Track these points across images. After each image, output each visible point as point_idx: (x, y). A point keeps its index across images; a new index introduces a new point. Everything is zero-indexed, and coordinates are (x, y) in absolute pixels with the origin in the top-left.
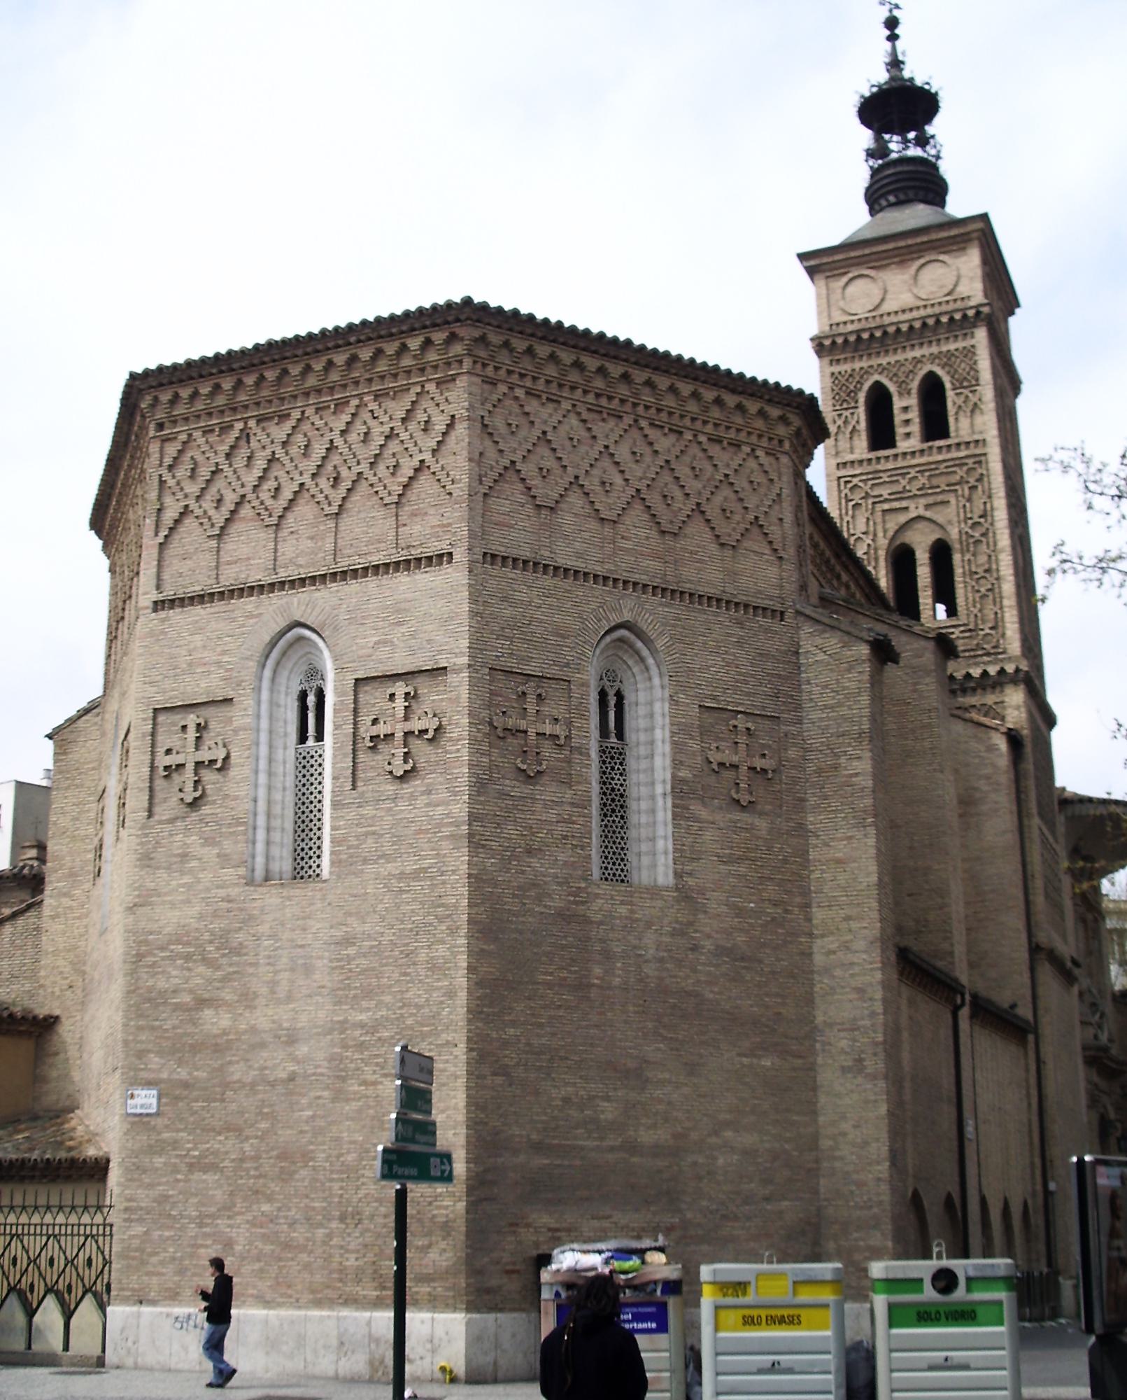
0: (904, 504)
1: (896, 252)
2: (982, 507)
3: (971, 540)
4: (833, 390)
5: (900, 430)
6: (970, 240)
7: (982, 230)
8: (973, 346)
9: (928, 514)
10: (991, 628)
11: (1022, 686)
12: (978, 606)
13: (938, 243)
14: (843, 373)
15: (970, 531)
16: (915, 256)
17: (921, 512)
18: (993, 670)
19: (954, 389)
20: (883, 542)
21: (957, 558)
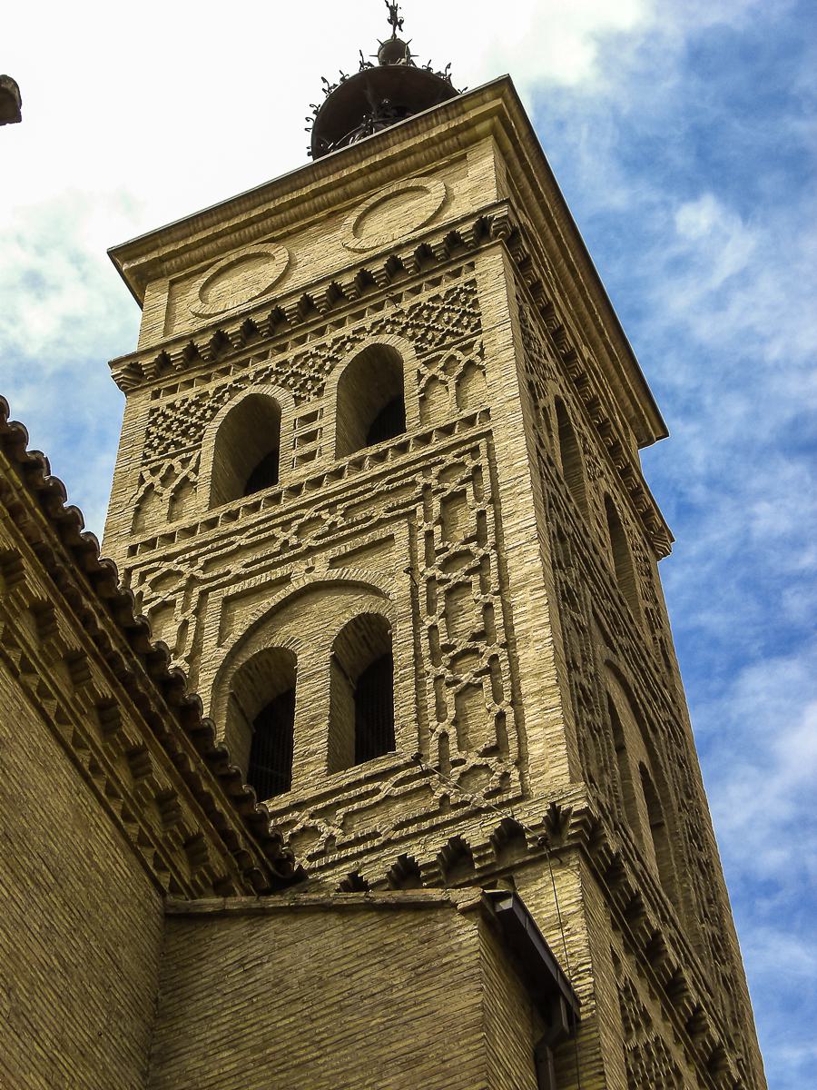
0: (280, 572)
1: (318, 200)
2: (473, 522)
3: (441, 589)
4: (149, 434)
5: (288, 450)
6: (476, 140)
7: (498, 112)
8: (473, 282)
9: (335, 574)
10: (487, 752)
11: (575, 859)
12: (451, 713)
13: (411, 160)
14: (178, 404)
15: (438, 573)
16: (359, 198)
17: (322, 572)
18: (477, 834)
19: (419, 358)
20: (213, 654)
21: (402, 631)
